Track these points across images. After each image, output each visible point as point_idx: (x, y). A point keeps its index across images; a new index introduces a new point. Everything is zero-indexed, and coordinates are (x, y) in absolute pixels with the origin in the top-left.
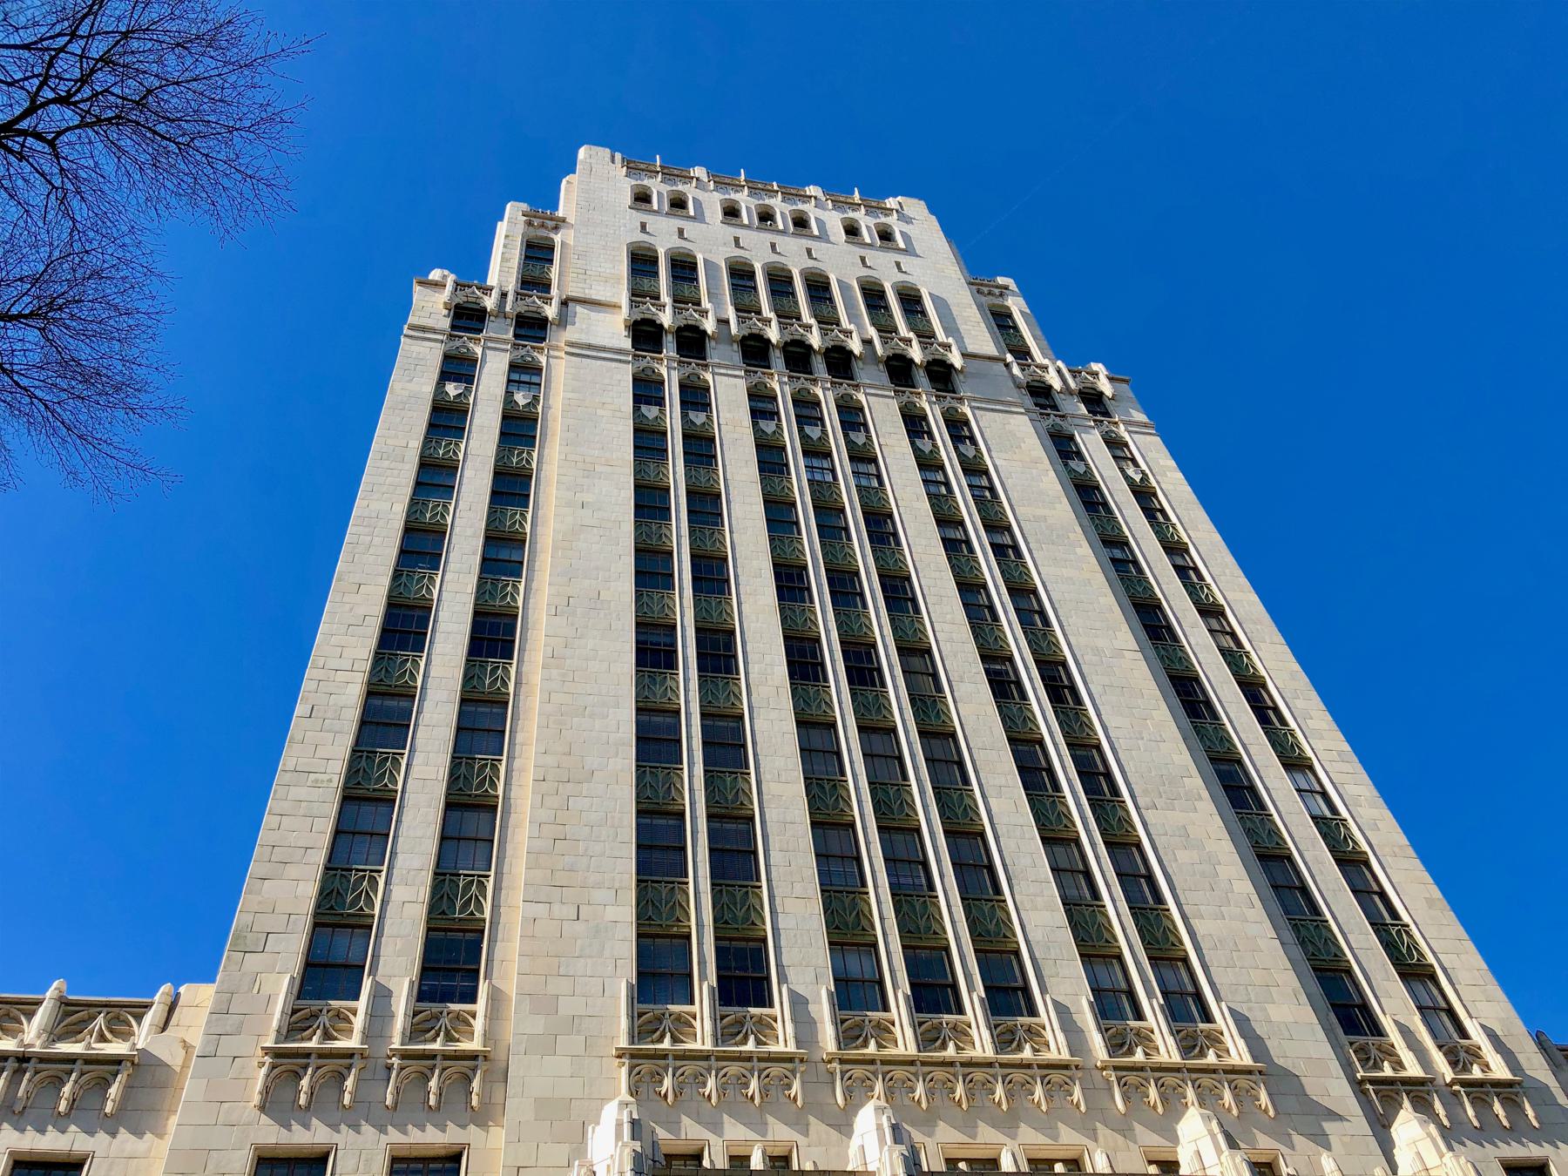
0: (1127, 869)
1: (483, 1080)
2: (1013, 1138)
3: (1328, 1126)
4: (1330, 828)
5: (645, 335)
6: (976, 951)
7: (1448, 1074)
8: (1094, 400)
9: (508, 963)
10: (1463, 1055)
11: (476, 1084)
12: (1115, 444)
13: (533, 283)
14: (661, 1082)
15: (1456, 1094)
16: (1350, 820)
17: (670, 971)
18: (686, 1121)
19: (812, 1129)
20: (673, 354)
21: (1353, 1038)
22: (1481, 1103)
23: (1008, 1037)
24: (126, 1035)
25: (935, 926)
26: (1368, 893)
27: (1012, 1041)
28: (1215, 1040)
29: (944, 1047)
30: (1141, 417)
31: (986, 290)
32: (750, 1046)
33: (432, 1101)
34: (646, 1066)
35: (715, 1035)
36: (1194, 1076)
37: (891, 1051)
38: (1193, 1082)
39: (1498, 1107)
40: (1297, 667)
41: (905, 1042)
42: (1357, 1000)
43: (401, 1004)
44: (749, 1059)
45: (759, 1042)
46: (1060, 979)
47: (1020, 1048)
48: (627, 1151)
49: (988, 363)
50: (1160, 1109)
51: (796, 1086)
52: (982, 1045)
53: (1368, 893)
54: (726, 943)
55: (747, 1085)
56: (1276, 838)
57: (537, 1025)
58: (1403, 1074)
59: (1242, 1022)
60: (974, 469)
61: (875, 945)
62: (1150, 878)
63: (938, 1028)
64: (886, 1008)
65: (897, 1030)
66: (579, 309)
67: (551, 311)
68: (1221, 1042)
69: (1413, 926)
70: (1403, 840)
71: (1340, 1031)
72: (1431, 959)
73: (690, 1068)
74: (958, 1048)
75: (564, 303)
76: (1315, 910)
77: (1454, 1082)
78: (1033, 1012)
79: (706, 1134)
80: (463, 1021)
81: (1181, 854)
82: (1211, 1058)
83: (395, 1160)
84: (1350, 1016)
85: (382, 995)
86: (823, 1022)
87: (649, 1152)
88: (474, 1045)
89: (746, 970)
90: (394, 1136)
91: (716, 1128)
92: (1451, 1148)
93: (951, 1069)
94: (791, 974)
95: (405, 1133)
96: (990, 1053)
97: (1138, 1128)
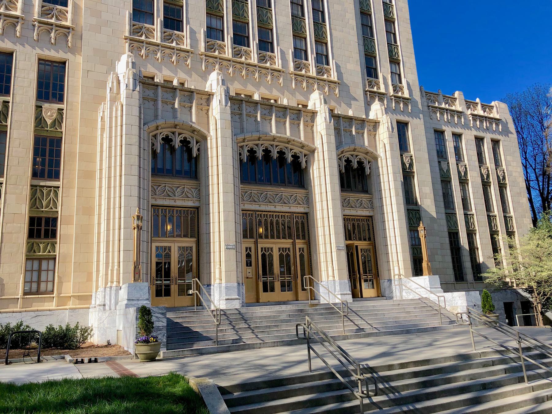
0: (316, 8)
1: (73, 38)
2: (258, 90)
3: (352, 102)
6: (258, 26)
7: (391, 92)
10: (398, 88)
11: (70, 38)
14: (141, 51)
15: (391, 99)
16: (394, 6)
17: (145, 11)
18: (149, 66)
19: (193, 76)
21: (369, 78)
22: (397, 103)
23: (263, 58)
25: (245, 15)
26: (390, 33)
27: (264, 60)
28: (328, 71)
29: (241, 57)
32: (174, 44)
33: (53, 41)
34: (136, 44)
35: (161, 38)
36: (319, 81)
37: (223, 56)
38: (318, 83)
39: (402, 105)
41: (228, 53)
42: (374, 67)
44: (173, 49)
45: (177, 44)
47: (266, 62)
48: (131, 72)
50: (305, 90)
51: (189, 61)
52: (254, 59)
53: (390, 33)
54: (167, 5)
55: (172, 58)
56: (368, 7)
58: (379, 91)
59: (338, 67)
61: (223, 17)
62: (323, 13)
63: (240, 51)
64: (223, 40)
65: (226, 49)
68: (329, 72)
69: (399, 47)
70: (408, 17)
71: (366, 75)
72: (401, 58)
74: (246, 59)
76: (372, 35)
77: (392, 96)
78: (273, 51)
79: (156, 72)
82: (325, 77)
83: (39, 59)
84: (371, 71)
86: (201, 41)
87: (138, 73)
88: (68, 23)
89: (174, 17)
90: (39, 51)
91: (160, 70)
92: (386, 114)
93: (242, 65)
94: (191, 21)
95: (43, 51)
96: (256, 62)
97: (297, 94)
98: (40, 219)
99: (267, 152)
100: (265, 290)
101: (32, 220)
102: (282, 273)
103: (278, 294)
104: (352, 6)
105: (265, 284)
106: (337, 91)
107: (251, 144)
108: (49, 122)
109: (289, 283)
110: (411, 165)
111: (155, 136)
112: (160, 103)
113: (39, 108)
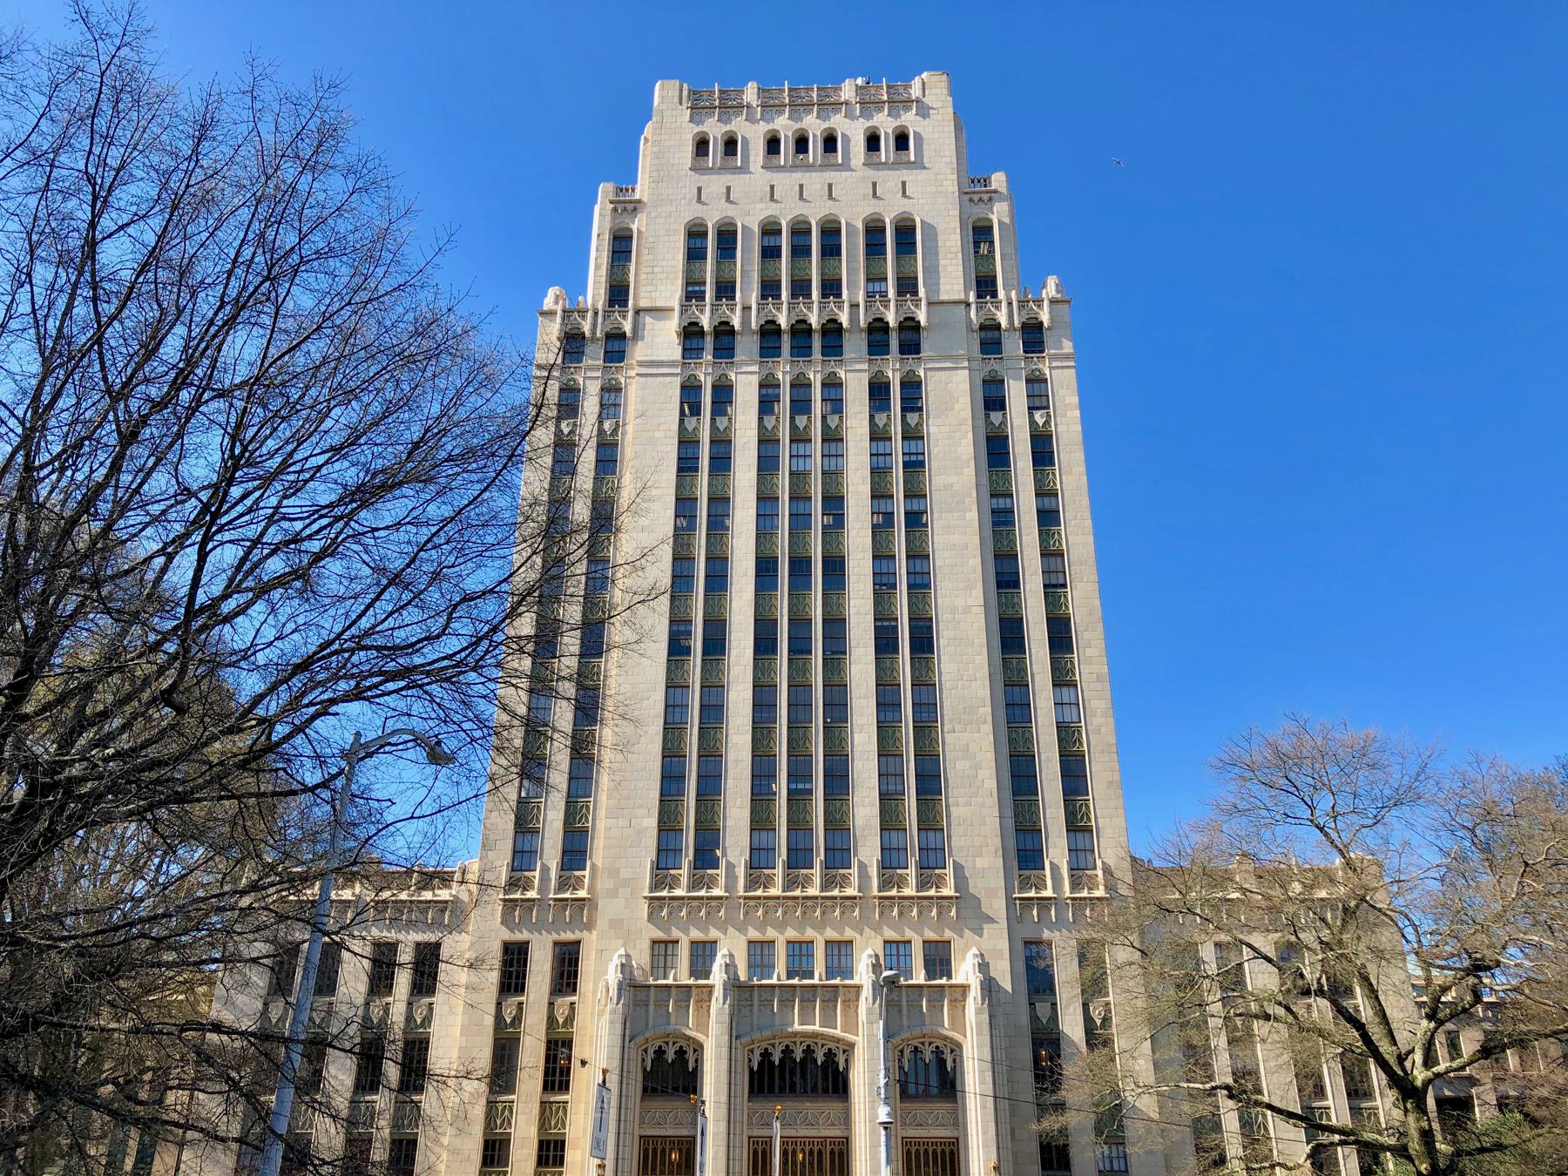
4: (1067, 734)
5: (691, 334)
8: (1033, 337)
9: (600, 851)
12: (1036, 382)
13: (618, 294)
20: (710, 357)
24: (450, 887)
30: (1068, 347)
31: (976, 197)
34: (656, 903)
40: (1097, 603)
43: (553, 875)
46: (868, 850)
49: (952, 307)
59: (958, 868)
60: (913, 435)
67: (627, 327)
73: (675, 903)
75: (637, 312)
80: (580, 880)
85: (545, 870)
91: (686, 931)
98: (549, 1142)
99: (787, 1051)
101: (541, 1143)
104: (991, 756)
107: (764, 1045)
108: (561, 1021)
110: (1106, 1020)
111: (646, 1051)
112: (652, 1007)
113: (551, 1004)
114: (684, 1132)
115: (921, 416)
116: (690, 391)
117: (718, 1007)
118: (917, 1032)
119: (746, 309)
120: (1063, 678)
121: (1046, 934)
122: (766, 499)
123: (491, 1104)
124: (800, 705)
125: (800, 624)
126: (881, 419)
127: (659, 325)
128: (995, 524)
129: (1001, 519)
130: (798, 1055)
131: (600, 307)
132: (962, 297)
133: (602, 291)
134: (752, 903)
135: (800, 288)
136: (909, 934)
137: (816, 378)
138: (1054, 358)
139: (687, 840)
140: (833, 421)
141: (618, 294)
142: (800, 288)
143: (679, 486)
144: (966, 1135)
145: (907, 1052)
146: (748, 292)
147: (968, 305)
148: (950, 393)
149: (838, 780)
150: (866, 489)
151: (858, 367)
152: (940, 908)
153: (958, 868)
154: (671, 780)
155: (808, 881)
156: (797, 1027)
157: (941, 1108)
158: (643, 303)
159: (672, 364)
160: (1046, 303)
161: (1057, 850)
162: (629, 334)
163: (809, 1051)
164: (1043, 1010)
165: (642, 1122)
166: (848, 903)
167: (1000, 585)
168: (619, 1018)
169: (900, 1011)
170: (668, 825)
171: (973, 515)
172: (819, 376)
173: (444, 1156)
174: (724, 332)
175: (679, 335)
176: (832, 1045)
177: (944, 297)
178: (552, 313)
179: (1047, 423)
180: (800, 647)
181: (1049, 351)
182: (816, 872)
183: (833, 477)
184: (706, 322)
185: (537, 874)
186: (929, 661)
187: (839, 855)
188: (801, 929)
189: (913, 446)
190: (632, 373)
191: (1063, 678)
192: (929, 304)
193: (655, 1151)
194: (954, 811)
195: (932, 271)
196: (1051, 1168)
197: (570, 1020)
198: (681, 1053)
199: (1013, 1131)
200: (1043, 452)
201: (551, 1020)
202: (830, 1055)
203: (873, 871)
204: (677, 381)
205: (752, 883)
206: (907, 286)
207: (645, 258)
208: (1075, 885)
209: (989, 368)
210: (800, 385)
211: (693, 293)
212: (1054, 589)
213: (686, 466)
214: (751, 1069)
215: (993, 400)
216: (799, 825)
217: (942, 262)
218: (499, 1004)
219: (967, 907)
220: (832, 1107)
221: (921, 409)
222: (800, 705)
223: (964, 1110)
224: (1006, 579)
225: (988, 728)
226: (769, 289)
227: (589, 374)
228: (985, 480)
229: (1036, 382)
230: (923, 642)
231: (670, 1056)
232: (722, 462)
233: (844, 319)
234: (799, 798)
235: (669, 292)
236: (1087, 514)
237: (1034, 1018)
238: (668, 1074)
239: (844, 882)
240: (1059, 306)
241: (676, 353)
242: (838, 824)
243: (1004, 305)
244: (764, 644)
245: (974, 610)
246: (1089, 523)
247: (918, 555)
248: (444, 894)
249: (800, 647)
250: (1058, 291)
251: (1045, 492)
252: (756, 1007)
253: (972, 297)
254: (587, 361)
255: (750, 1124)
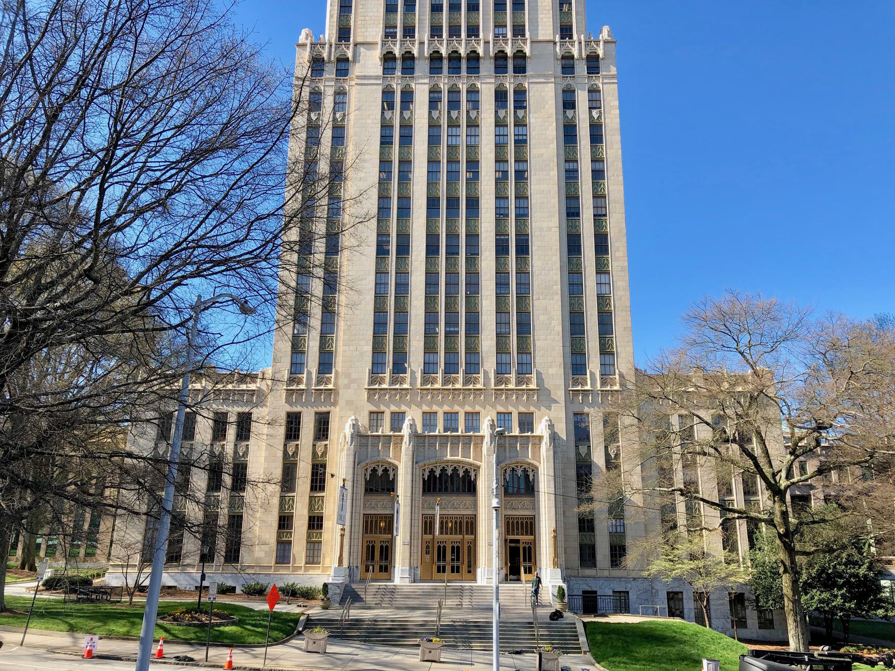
4: (603, 300)
5: (388, 58)
8: (593, 63)
9: (339, 363)
12: (594, 91)
13: (344, 33)
20: (399, 74)
24: (255, 382)
30: (613, 70)
34: (372, 392)
40: (624, 225)
43: (314, 376)
46: (489, 363)
57: (346, 381)
59: (539, 374)
60: (520, 123)
66: (362, 49)
67: (350, 54)
73: (382, 392)
75: (356, 45)
80: (329, 379)
81: (542, 318)
85: (309, 373)
91: (388, 407)
98: (314, 517)
99: (443, 470)
100: (439, 571)
101: (310, 518)
102: (453, 560)
103: (447, 574)
104: (559, 313)
105: (439, 568)
106: (535, 398)
107: (431, 467)
108: (320, 454)
109: (458, 567)
110: (617, 455)
112: (370, 447)
113: (314, 445)
114: (388, 512)
115: (525, 112)
116: (387, 94)
117: (406, 447)
118: (514, 461)
119: (422, 43)
120: (602, 269)
121: (586, 410)
122: (433, 162)
123: (282, 498)
124: (452, 284)
125: (452, 237)
126: (502, 113)
127: (369, 53)
128: (567, 178)
129: (571, 175)
130: (449, 472)
131: (333, 42)
132: (552, 38)
133: (334, 32)
134: (425, 392)
135: (454, 31)
136: (511, 409)
137: (463, 87)
138: (605, 77)
139: (387, 356)
140: (473, 114)
141: (344, 33)
142: (454, 31)
143: (381, 154)
144: (539, 514)
145: (508, 471)
146: (423, 33)
147: (555, 43)
148: (543, 97)
149: (473, 326)
150: (492, 156)
151: (488, 80)
152: (528, 395)
153: (539, 374)
154: (379, 325)
155: (456, 380)
156: (449, 457)
157: (526, 500)
158: (359, 40)
159: (377, 78)
160: (601, 43)
161: (594, 364)
162: (350, 59)
163: (455, 470)
164: (583, 450)
165: (365, 506)
166: (478, 392)
167: (568, 215)
168: (352, 452)
169: (505, 449)
170: (378, 350)
171: (554, 173)
172: (465, 86)
173: (258, 523)
174: (408, 58)
175: (381, 60)
176: (468, 467)
177: (540, 38)
178: (304, 45)
179: (599, 117)
180: (452, 251)
181: (603, 73)
182: (461, 375)
183: (473, 148)
184: (397, 51)
185: (305, 375)
186: (526, 259)
187: (473, 367)
188: (451, 406)
189: (521, 130)
190: (353, 83)
191: (602, 269)
192: (532, 42)
193: (371, 522)
194: (538, 343)
195: (534, 22)
196: (584, 531)
197: (324, 454)
198: (386, 471)
199: (564, 512)
200: (596, 136)
201: (314, 454)
202: (467, 472)
203: (492, 375)
204: (380, 88)
205: (425, 381)
206: (519, 31)
207: (360, 10)
208: (603, 383)
209: (566, 83)
210: (454, 92)
211: (389, 34)
212: (599, 217)
213: (386, 141)
214: (424, 479)
215: (569, 103)
216: (451, 350)
217: (540, 16)
218: (285, 445)
219: (543, 395)
220: (467, 499)
221: (525, 108)
222: (452, 284)
223: (539, 501)
224: (572, 212)
225: (558, 297)
226: (436, 31)
227: (327, 84)
228: (562, 152)
229: (594, 91)
230: (523, 248)
231: (380, 472)
232: (407, 139)
233: (480, 51)
234: (451, 336)
235: (376, 33)
236: (621, 173)
237: (578, 454)
238: (379, 482)
239: (476, 381)
240: (609, 45)
241: (379, 71)
242: (472, 350)
243: (576, 44)
244: (432, 249)
245: (553, 229)
246: (621, 178)
247: (522, 197)
248: (253, 387)
249: (452, 251)
250: (609, 36)
251: (596, 159)
252: (426, 447)
253: (558, 39)
254: (326, 75)
255: (423, 508)
